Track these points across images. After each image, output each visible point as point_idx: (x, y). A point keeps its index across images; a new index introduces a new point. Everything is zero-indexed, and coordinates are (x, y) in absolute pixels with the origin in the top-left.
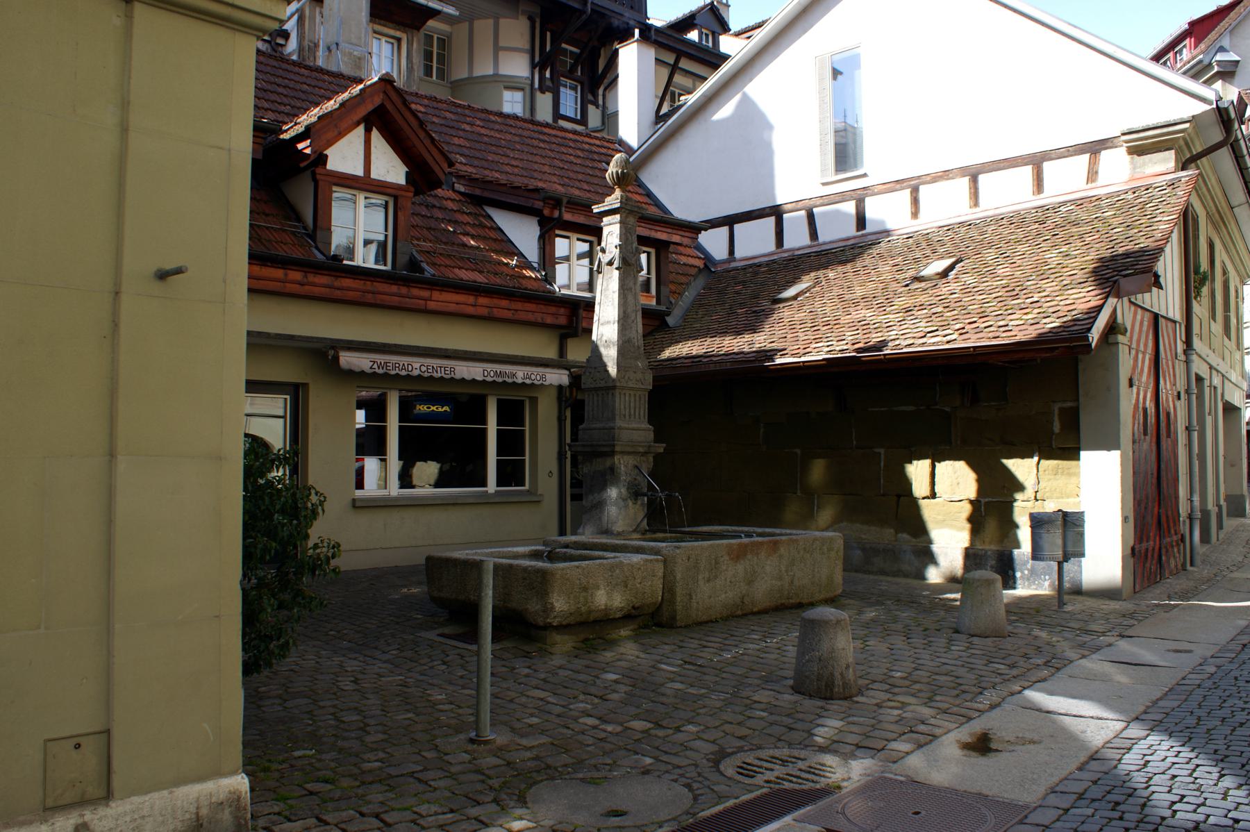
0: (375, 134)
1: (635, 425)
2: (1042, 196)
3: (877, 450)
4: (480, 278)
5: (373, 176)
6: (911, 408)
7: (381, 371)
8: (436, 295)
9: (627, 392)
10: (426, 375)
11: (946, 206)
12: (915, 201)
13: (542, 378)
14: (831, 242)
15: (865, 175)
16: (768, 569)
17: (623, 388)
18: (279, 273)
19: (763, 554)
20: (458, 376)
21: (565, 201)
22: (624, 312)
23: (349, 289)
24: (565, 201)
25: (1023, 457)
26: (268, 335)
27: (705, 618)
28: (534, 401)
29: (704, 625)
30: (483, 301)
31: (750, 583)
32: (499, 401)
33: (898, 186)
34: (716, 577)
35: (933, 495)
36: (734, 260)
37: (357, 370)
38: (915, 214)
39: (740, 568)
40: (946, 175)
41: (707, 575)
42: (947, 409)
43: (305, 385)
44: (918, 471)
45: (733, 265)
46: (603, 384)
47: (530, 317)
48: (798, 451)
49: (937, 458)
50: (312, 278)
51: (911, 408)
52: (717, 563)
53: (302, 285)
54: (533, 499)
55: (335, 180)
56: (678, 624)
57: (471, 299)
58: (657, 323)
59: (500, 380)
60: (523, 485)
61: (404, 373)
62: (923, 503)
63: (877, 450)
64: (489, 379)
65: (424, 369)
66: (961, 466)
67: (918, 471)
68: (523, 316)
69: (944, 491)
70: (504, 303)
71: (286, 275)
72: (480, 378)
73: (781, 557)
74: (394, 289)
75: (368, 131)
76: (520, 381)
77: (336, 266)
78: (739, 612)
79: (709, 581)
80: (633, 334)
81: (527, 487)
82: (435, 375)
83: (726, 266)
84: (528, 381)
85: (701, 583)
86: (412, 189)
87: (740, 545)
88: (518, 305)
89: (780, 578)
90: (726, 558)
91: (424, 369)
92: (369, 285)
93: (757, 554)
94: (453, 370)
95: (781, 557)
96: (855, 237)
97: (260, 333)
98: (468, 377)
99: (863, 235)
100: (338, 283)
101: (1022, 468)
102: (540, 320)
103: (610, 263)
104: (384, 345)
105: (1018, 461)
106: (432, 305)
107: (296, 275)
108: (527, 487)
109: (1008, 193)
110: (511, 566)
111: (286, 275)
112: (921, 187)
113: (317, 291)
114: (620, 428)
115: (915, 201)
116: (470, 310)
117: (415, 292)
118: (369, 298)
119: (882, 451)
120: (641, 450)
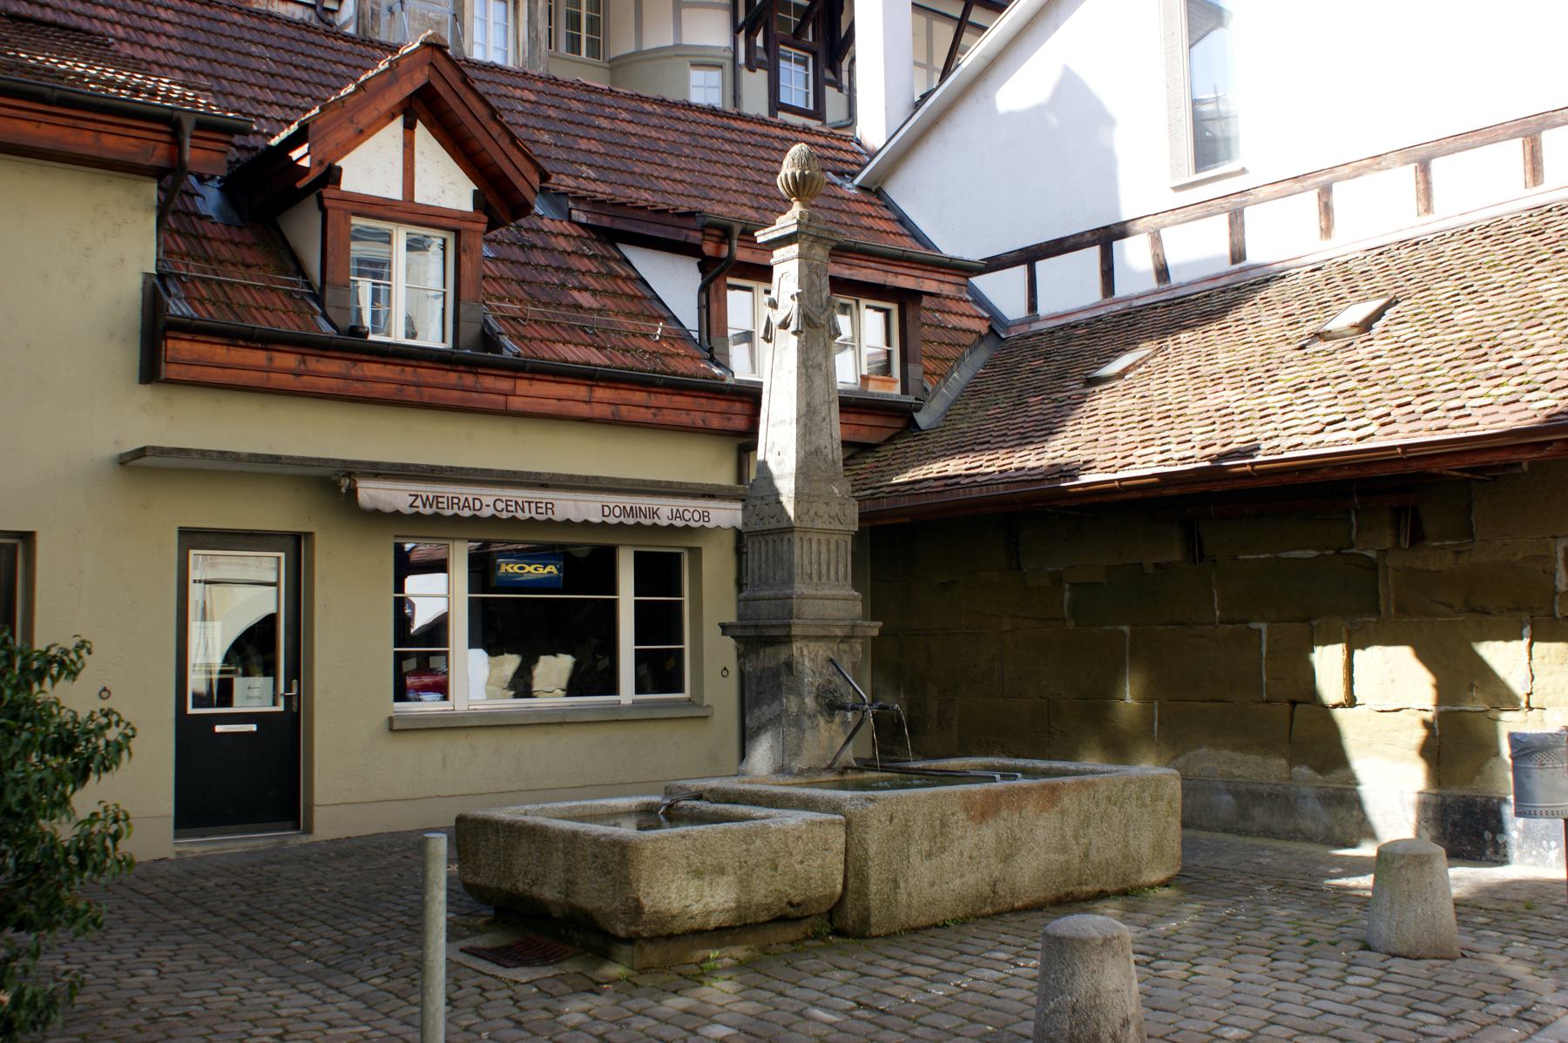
0: (421, 131)
1: (827, 592)
2: (1540, 188)
3: (1254, 625)
4: (596, 358)
5: (417, 199)
6: (1311, 553)
7: (428, 511)
8: (523, 386)
9: (815, 537)
10: (505, 515)
11: (1378, 214)
12: (1326, 210)
13: (702, 516)
14: (1189, 284)
15: (1243, 171)
16: (1041, 834)
17: (807, 530)
18: (259, 357)
19: (1030, 810)
20: (559, 516)
22: (808, 405)
25: (1507, 638)
26: (236, 457)
27: (923, 920)
28: (696, 553)
29: (918, 932)
30: (601, 393)
31: (1007, 858)
32: (639, 557)
33: (1297, 186)
34: (943, 849)
35: (1351, 701)
36: (1037, 319)
37: (388, 509)
38: (1327, 231)
39: (988, 833)
40: (1377, 161)
41: (926, 846)
42: (1371, 554)
43: (309, 535)
44: (1327, 661)
45: (1036, 327)
46: (773, 525)
47: (684, 419)
48: (1126, 629)
49: (1356, 641)
50: (313, 364)
51: (1311, 553)
52: (943, 825)
54: (697, 713)
55: (356, 207)
56: (874, 931)
57: (582, 392)
58: (899, 423)
59: (631, 521)
60: (680, 690)
61: (466, 513)
62: (1339, 713)
63: (1254, 625)
64: (612, 520)
65: (500, 506)
66: (1403, 655)
67: (1327, 661)
68: (669, 417)
69: (1379, 698)
70: (639, 397)
72: (596, 519)
73: (1063, 812)
74: (452, 378)
75: (409, 127)
76: (664, 522)
77: (353, 343)
78: (988, 909)
79: (929, 856)
80: (824, 441)
81: (687, 694)
82: (520, 515)
83: (1024, 329)
84: (679, 523)
85: (915, 860)
86: (485, 218)
87: (987, 794)
88: (663, 400)
89: (1064, 849)
90: (962, 816)
91: (500, 506)
92: (409, 373)
93: (1020, 808)
94: (550, 506)
95: (1063, 812)
96: (1228, 274)
97: (222, 453)
98: (576, 517)
99: (1242, 270)
101: (1504, 657)
102: (700, 424)
103: (784, 325)
104: (433, 469)
105: (1500, 644)
106: (516, 403)
107: (288, 360)
108: (687, 694)
109: (1484, 187)
110: (575, 834)
112: (1335, 186)
113: (323, 384)
114: (802, 597)
115: (1326, 210)
116: (583, 410)
117: (488, 382)
118: (411, 394)
119: (1263, 626)
120: (838, 632)
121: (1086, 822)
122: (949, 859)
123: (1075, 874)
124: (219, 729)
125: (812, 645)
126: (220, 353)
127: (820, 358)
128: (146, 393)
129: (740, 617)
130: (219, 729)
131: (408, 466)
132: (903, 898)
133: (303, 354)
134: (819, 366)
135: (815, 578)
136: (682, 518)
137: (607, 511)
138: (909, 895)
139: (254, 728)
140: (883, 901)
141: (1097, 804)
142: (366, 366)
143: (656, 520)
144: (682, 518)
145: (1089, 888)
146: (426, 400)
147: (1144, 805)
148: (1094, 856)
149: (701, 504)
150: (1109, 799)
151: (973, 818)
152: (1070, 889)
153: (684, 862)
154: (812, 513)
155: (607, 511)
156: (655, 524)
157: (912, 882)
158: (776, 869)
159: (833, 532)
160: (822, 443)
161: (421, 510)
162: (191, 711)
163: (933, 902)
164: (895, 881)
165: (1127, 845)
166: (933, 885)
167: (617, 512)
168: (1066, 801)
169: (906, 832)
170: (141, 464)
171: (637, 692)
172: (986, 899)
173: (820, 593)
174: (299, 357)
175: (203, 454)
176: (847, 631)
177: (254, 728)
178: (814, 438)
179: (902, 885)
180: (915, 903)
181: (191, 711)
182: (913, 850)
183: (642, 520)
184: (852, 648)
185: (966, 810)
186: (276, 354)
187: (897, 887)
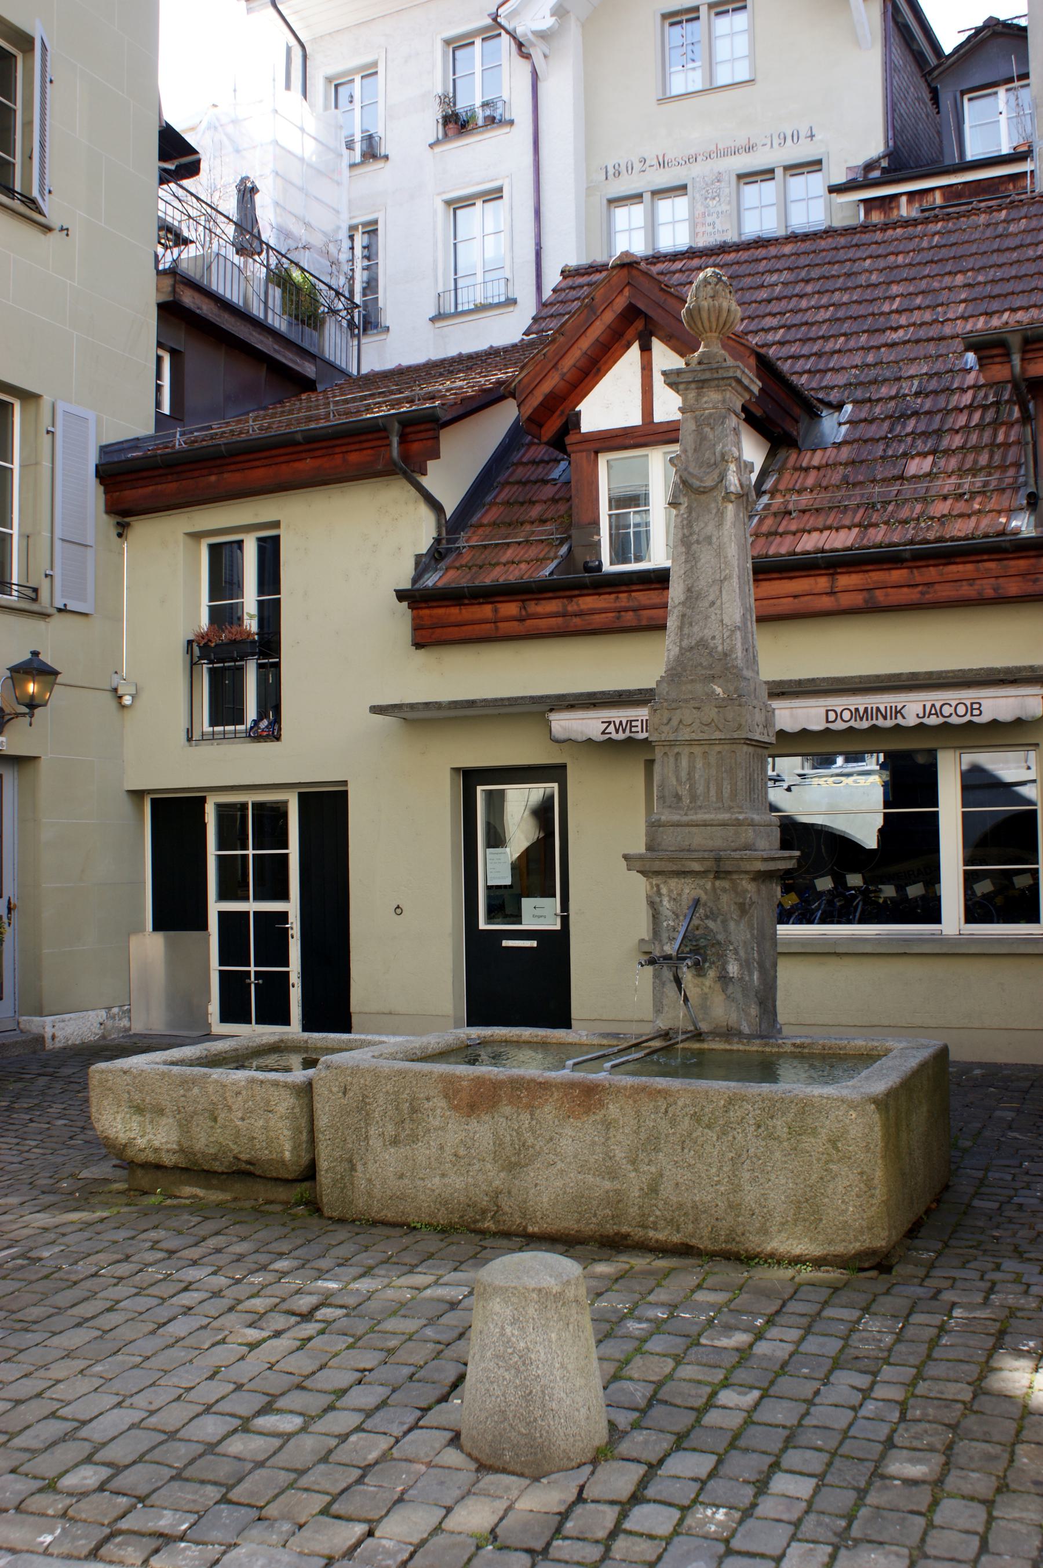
1: (701, 816)
4: (841, 540)
7: (621, 736)
9: (686, 751)
17: (672, 744)
18: (487, 611)
19: (548, 1112)
21: (1015, 341)
22: (689, 590)
23: (592, 612)
24: (1015, 341)
26: (438, 706)
27: (389, 1215)
30: (845, 581)
31: (512, 1167)
34: (414, 1138)
37: (580, 738)
39: (483, 1131)
41: (390, 1130)
43: (563, 767)
47: (966, 591)
50: (533, 608)
52: (414, 1110)
53: (521, 620)
57: (822, 583)
59: (865, 724)
68: (945, 592)
70: (897, 575)
71: (496, 611)
72: (818, 726)
73: (608, 1125)
76: (911, 721)
78: (488, 1224)
79: (395, 1142)
84: (933, 721)
85: (376, 1143)
87: (479, 1082)
88: (932, 573)
89: (612, 1174)
90: (440, 1103)
93: (531, 1108)
95: (608, 1125)
97: (427, 704)
100: (572, 608)
102: (989, 593)
104: (620, 694)
107: (511, 609)
111: (496, 611)
113: (543, 624)
116: (827, 603)
118: (629, 618)
120: (696, 867)
121: (653, 1143)
122: (423, 1152)
123: (634, 1211)
124: (506, 943)
125: (673, 883)
126: (454, 613)
127: (710, 529)
128: (421, 657)
129: (649, 848)
130: (506, 943)
131: (595, 693)
132: (362, 1184)
133: (523, 601)
134: (709, 539)
135: (686, 801)
136: (939, 713)
137: (832, 716)
138: (370, 1180)
139: (534, 944)
140: (335, 1182)
141: (673, 1123)
142: (588, 599)
143: (900, 720)
144: (939, 713)
145: (661, 1236)
146: (644, 623)
147: (770, 1136)
148: (666, 1190)
149: (968, 695)
150: (696, 1118)
151: (456, 1108)
152: (625, 1229)
153: (126, 1096)
154: (674, 722)
155: (832, 716)
156: (897, 725)
157: (372, 1167)
158: (215, 1120)
159: (711, 742)
160: (708, 633)
161: (614, 736)
162: (483, 925)
163: (403, 1198)
164: (350, 1161)
165: (737, 1189)
166: (401, 1177)
167: (846, 715)
168: (613, 1110)
169: (363, 1106)
170: (420, 718)
171: (968, 920)
172: (484, 1212)
173: (685, 819)
174: (519, 604)
175: (427, 705)
176: (709, 865)
177: (534, 944)
178: (696, 629)
179: (360, 1167)
180: (377, 1192)
181: (483, 925)
182: (372, 1131)
183: (880, 722)
184: (734, 888)
185: (446, 1096)
186: (499, 605)
187: (353, 1168)
